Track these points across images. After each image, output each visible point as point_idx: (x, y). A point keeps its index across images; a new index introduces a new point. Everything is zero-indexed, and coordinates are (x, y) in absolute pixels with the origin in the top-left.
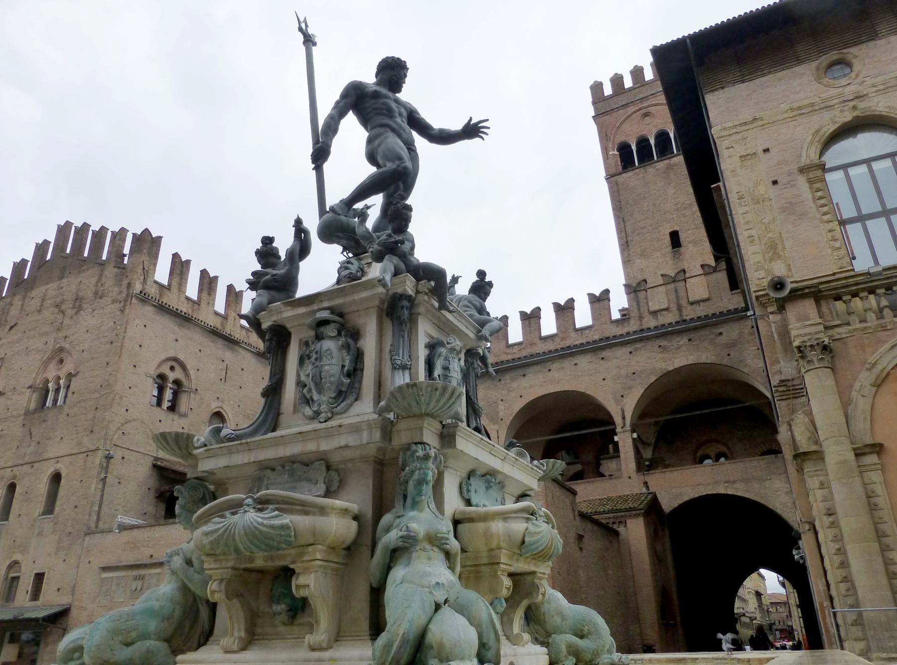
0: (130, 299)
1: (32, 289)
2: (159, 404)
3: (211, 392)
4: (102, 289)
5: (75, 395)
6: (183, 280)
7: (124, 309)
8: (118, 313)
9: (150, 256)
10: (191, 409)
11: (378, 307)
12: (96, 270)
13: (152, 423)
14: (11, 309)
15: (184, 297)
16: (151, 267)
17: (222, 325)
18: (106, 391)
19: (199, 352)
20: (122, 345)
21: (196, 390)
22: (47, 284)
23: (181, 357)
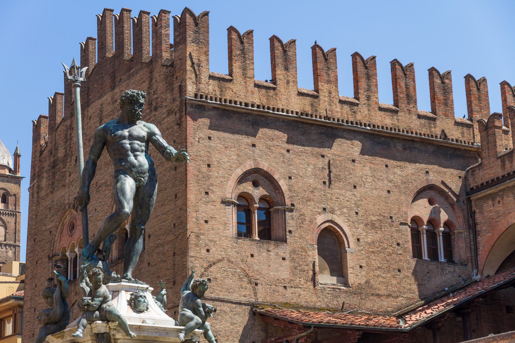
0: (184, 107)
1: (88, 106)
2: (248, 234)
3: (313, 203)
4: (156, 96)
5: (151, 238)
6: (248, 62)
7: (181, 122)
8: (176, 127)
9: (198, 43)
10: (290, 232)
11: (91, 340)
12: (144, 73)
13: (242, 260)
14: (72, 135)
15: (252, 85)
16: (203, 58)
17: (312, 105)
18: (181, 231)
19: (286, 153)
20: (186, 170)
21: (293, 205)
22: (100, 97)
23: (264, 166)
